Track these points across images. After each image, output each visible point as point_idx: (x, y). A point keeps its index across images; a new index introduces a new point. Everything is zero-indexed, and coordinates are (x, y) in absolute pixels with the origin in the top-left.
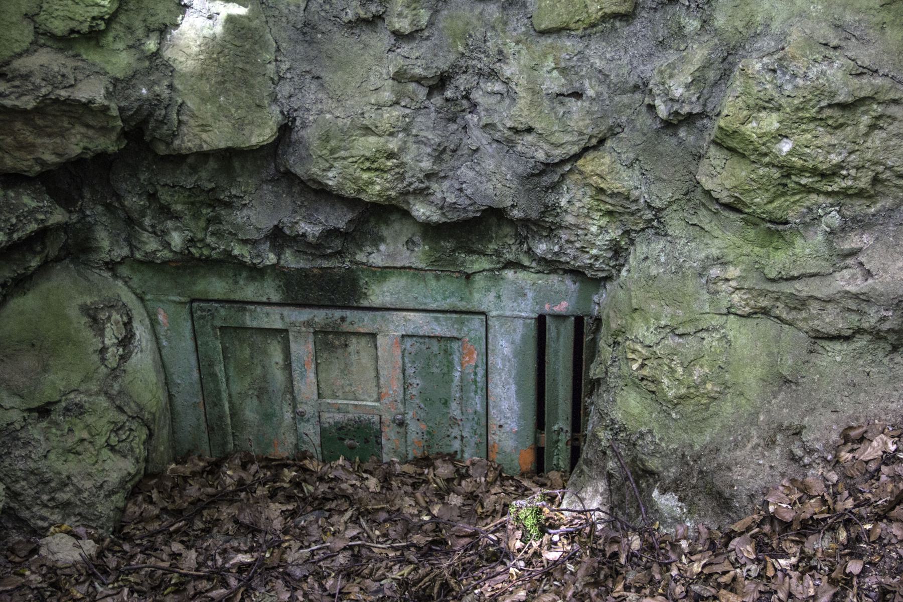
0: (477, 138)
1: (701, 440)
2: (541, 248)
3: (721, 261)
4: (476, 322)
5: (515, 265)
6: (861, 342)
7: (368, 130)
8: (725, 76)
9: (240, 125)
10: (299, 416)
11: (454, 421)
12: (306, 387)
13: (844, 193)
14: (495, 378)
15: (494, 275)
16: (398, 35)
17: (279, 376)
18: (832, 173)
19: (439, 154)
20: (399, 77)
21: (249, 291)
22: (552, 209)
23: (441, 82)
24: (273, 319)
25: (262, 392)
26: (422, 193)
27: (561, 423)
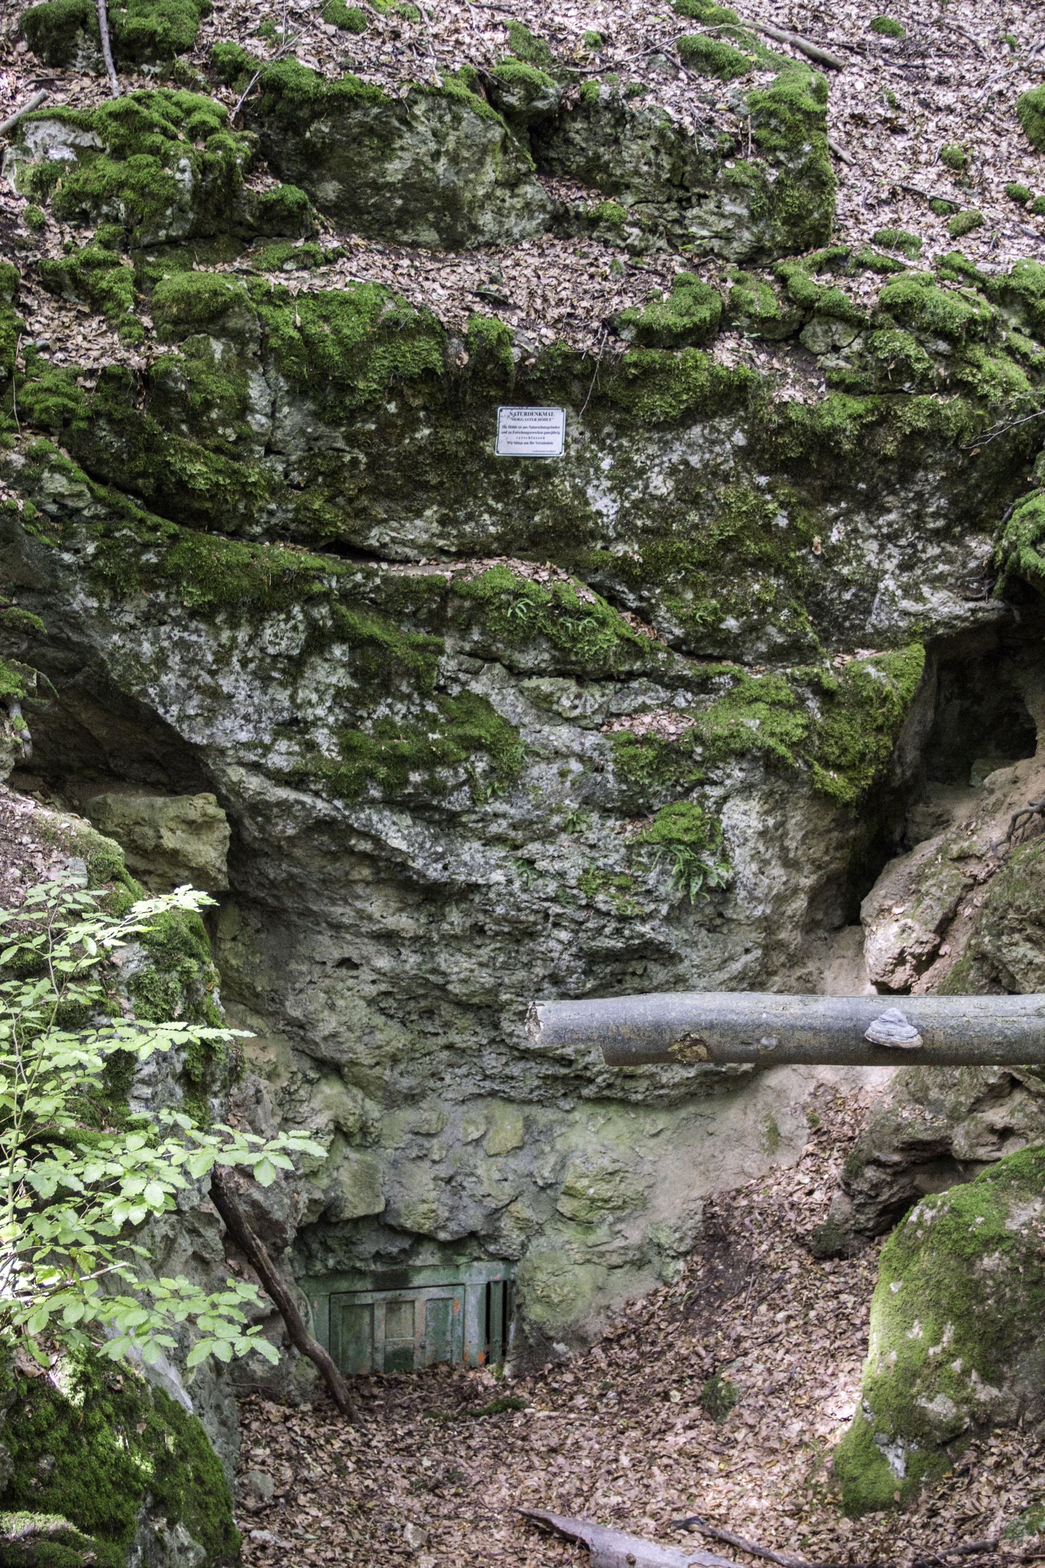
0: (466, 1201)
1: (570, 1319)
2: (492, 1248)
3: (569, 1242)
4: (460, 1289)
5: (478, 1259)
6: (627, 1267)
7: (424, 1201)
8: (563, 1167)
9: (369, 1205)
10: (375, 1349)
11: (448, 1343)
12: (380, 1334)
13: (614, 1208)
14: (468, 1317)
15: (469, 1265)
16: (434, 1162)
17: (367, 1329)
18: (606, 1201)
19: (452, 1209)
20: (435, 1179)
21: (359, 1286)
22: (498, 1229)
23: (449, 1181)
24: (368, 1299)
25: (358, 1339)
26: (444, 1228)
27: (497, 1337)
